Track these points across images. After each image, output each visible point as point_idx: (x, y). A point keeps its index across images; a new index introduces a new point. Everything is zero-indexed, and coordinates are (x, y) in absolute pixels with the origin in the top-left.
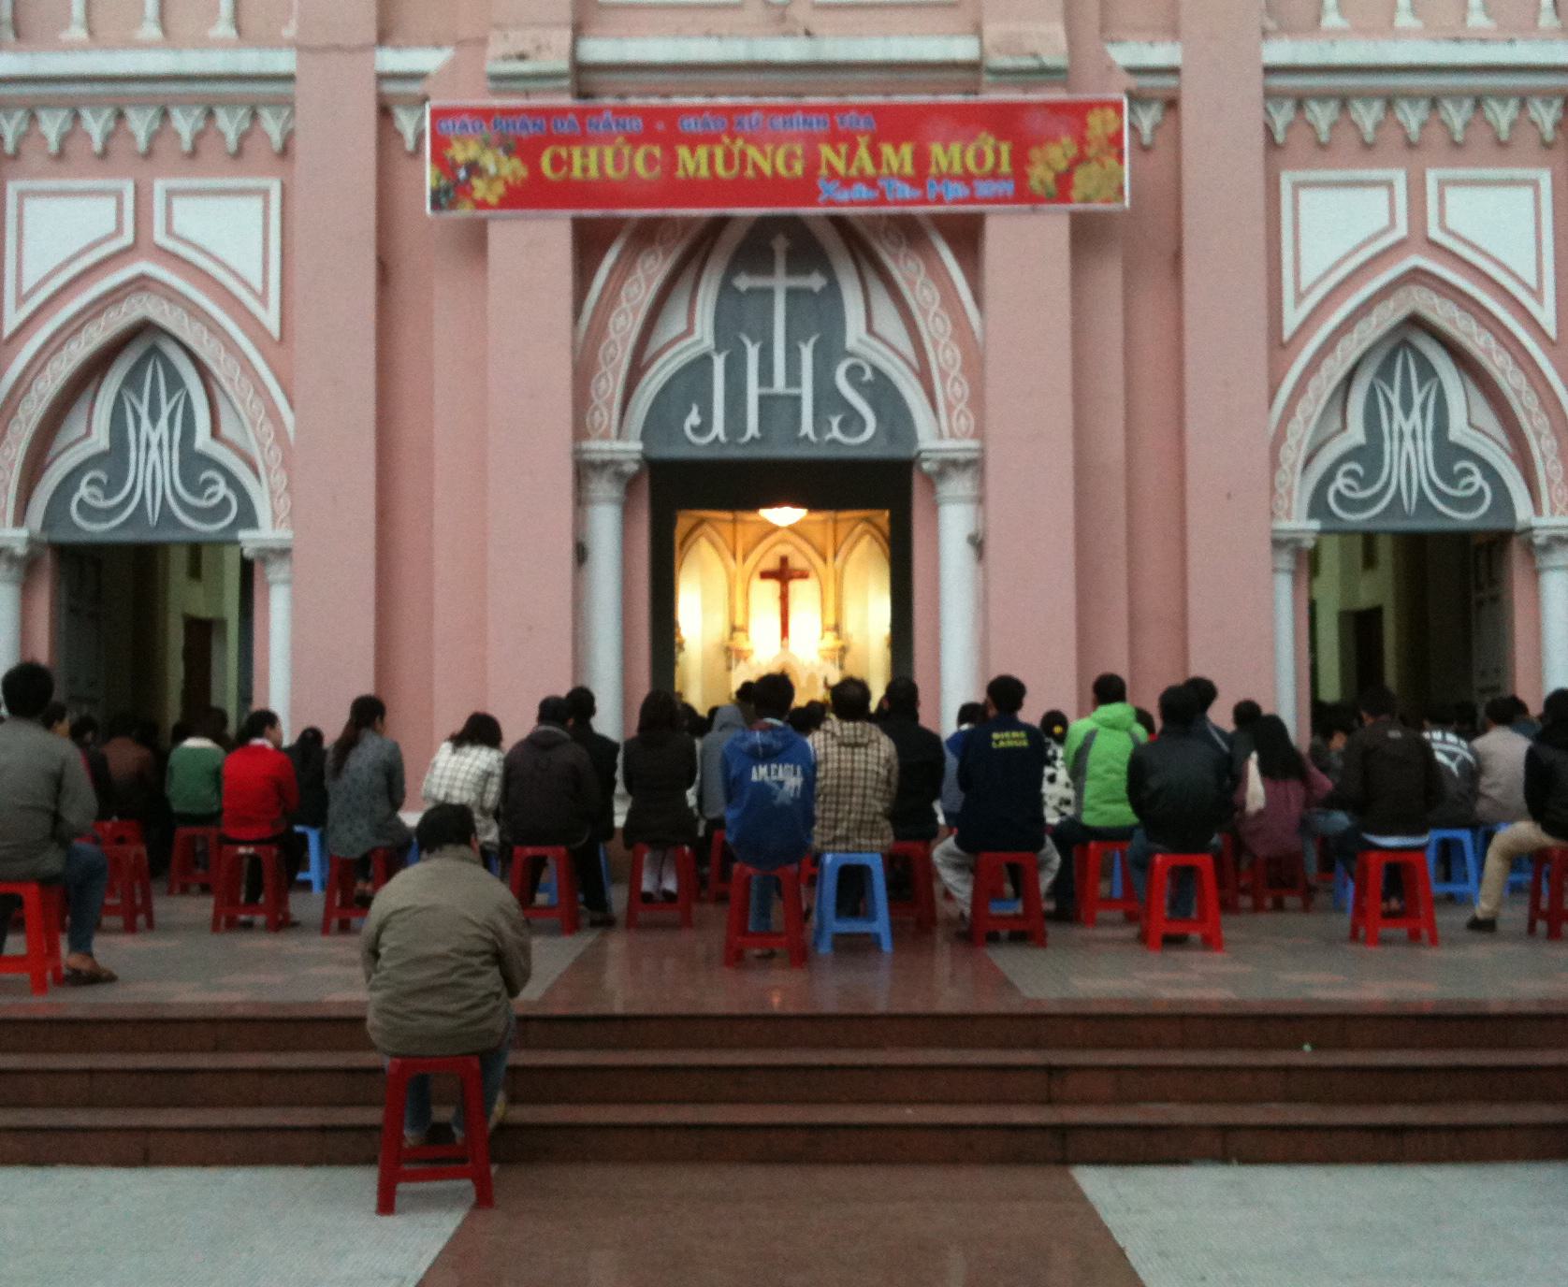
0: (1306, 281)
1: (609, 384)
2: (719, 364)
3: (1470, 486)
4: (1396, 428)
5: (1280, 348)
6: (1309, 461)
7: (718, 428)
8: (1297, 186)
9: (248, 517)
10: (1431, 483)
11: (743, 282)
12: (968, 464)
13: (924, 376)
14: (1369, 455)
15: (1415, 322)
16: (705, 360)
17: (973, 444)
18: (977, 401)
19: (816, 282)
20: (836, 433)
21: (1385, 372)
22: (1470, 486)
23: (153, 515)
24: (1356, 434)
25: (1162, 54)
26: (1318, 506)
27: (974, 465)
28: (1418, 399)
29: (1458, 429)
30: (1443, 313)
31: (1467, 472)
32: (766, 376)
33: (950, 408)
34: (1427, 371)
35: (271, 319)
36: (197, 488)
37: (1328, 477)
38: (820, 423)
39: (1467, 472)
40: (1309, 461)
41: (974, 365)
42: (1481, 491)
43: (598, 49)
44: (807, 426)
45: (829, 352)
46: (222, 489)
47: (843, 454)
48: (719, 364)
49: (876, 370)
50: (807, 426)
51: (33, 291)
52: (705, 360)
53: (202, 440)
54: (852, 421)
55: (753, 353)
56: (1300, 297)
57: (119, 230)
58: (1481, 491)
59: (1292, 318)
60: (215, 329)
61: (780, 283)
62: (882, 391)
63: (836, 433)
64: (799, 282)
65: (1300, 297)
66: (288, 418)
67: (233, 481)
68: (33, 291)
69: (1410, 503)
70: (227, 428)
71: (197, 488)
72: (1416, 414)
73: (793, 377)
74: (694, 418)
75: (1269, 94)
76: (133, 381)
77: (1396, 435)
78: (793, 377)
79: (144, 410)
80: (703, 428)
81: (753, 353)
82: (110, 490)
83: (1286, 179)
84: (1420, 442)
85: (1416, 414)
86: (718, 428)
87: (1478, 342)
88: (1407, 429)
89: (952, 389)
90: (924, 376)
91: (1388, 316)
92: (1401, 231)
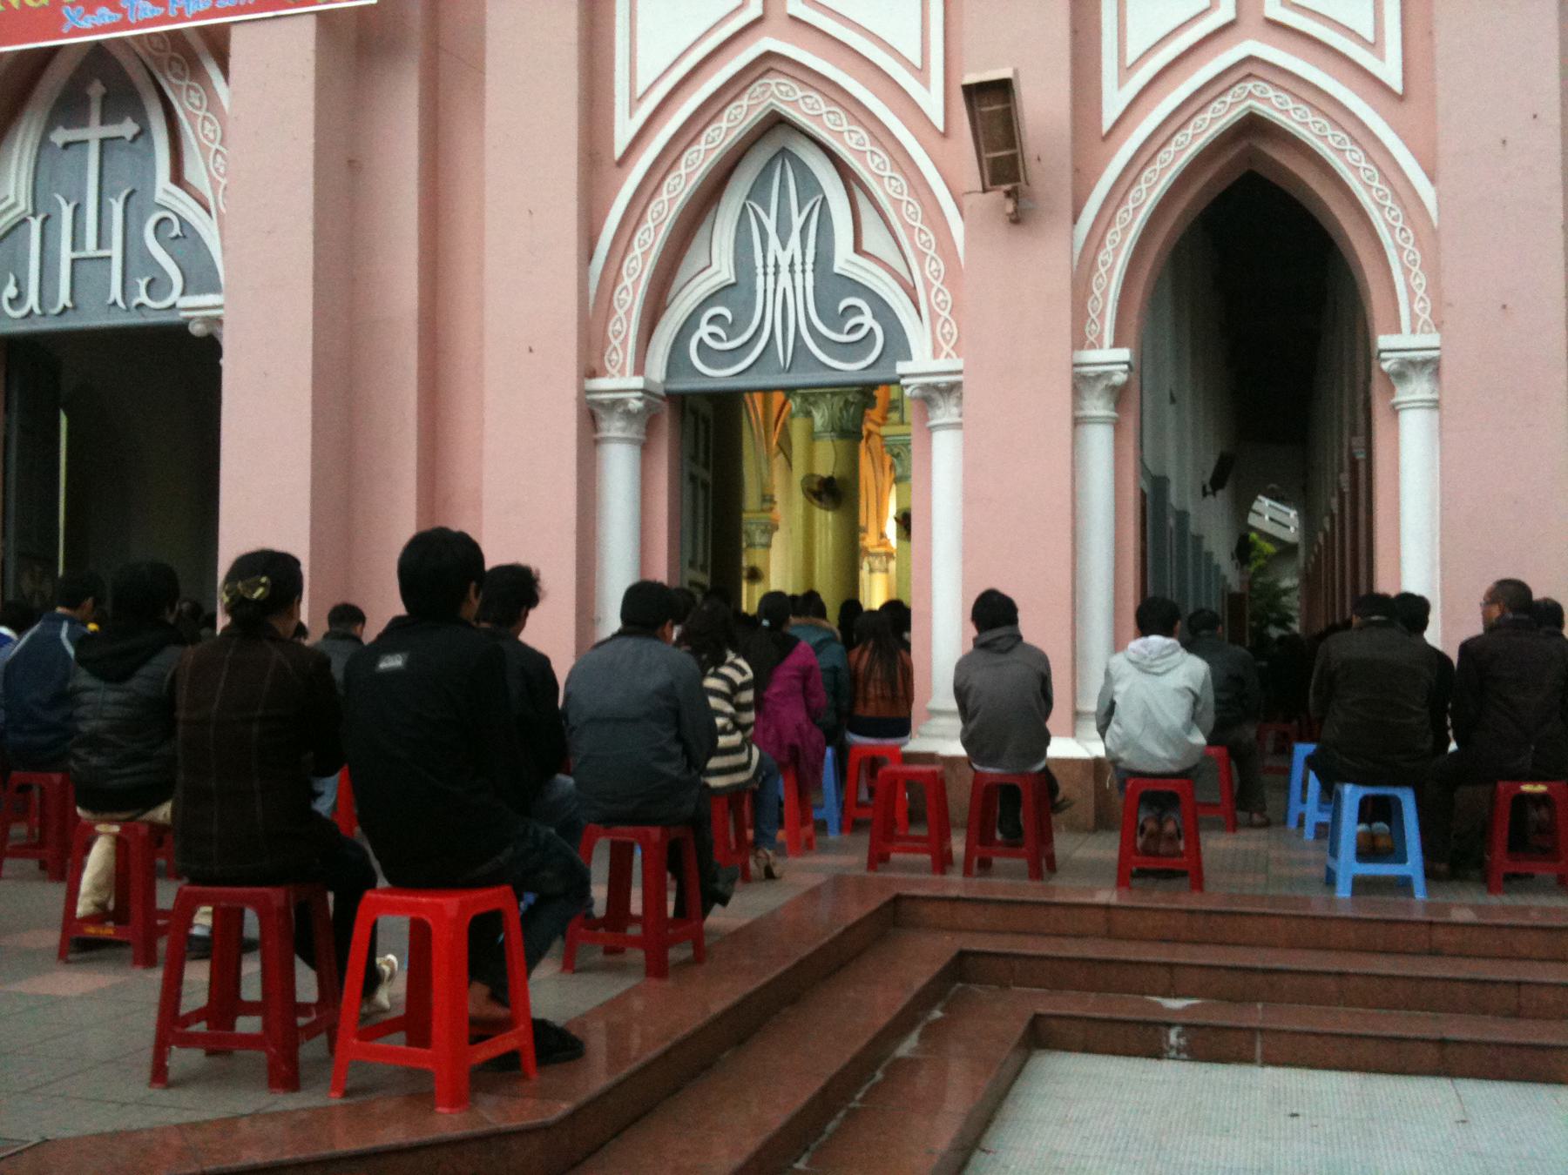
2: (35, 224)
3: (858, 326)
4: (771, 262)
7: (32, 300)
11: (60, 136)
14: (737, 293)
15: (775, 123)
19: (128, 128)
20: (143, 298)
21: (759, 191)
22: (858, 326)
24: (723, 270)
28: (797, 222)
29: (844, 260)
30: (804, 108)
31: (858, 311)
34: (808, 184)
37: (691, 323)
39: (853, 310)
42: (871, 330)
44: (116, 292)
47: (152, 319)
52: (25, 221)
54: (157, 285)
58: (871, 330)
61: (94, 133)
63: (143, 298)
64: (112, 131)
69: (784, 353)
74: (11, 291)
77: (771, 270)
80: (17, 301)
84: (798, 276)
86: (32, 300)
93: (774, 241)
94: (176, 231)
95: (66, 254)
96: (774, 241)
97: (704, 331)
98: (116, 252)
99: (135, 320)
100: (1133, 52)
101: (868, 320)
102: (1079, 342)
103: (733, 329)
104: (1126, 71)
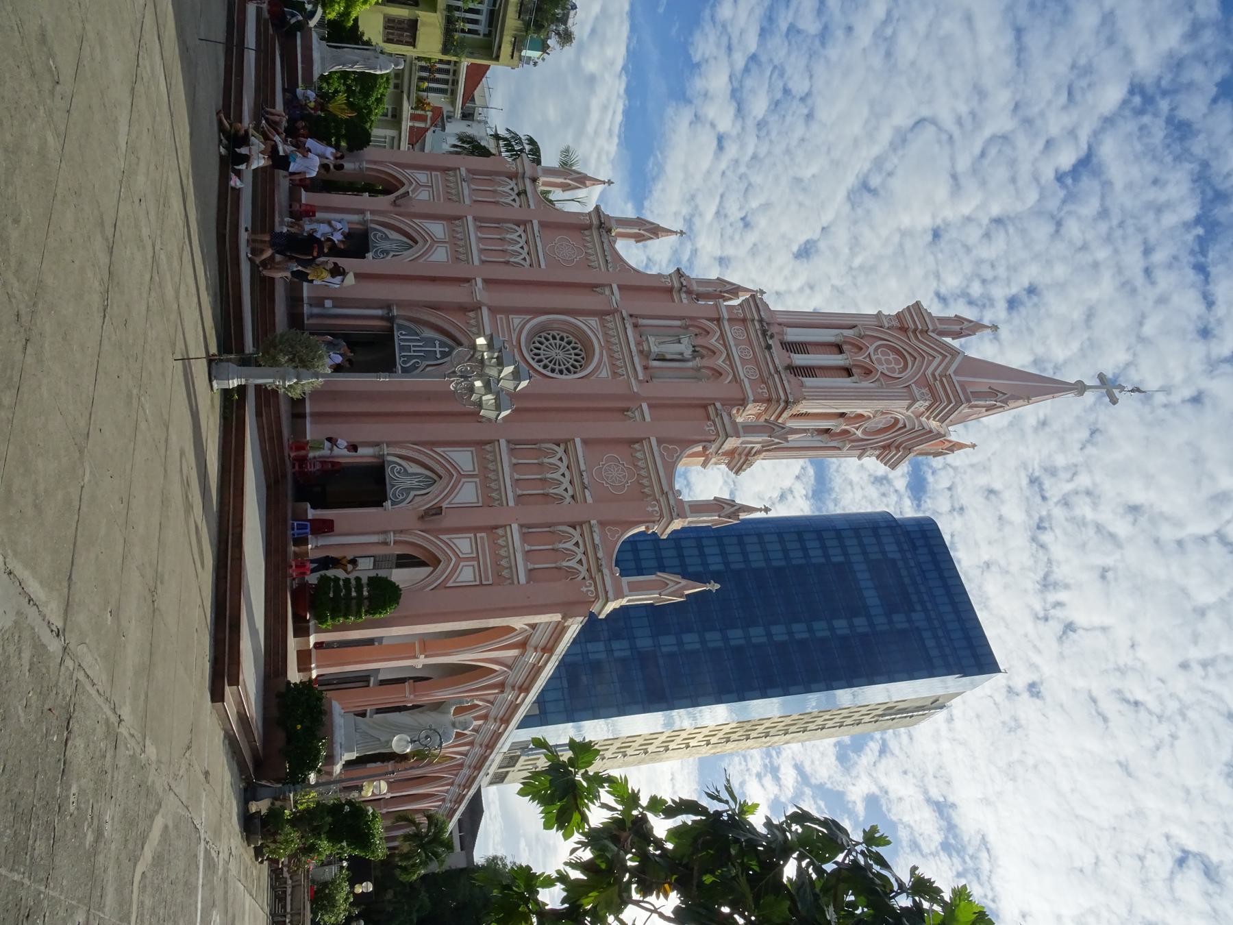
2: (418, 338)
7: (402, 337)
8: (472, 451)
11: (437, 343)
16: (418, 335)
32: (414, 346)
36: (382, 252)
38: (404, 356)
39: (403, 495)
43: (485, 311)
48: (418, 338)
54: (404, 362)
70: (418, 499)
73: (414, 351)
78: (414, 351)
80: (401, 334)
81: (421, 344)
86: (402, 337)
92: (463, 480)
95: (411, 344)
97: (398, 467)
98: (412, 354)
100: (454, 541)
101: (401, 498)
102: (395, 532)
103: (399, 473)
104: (450, 539)
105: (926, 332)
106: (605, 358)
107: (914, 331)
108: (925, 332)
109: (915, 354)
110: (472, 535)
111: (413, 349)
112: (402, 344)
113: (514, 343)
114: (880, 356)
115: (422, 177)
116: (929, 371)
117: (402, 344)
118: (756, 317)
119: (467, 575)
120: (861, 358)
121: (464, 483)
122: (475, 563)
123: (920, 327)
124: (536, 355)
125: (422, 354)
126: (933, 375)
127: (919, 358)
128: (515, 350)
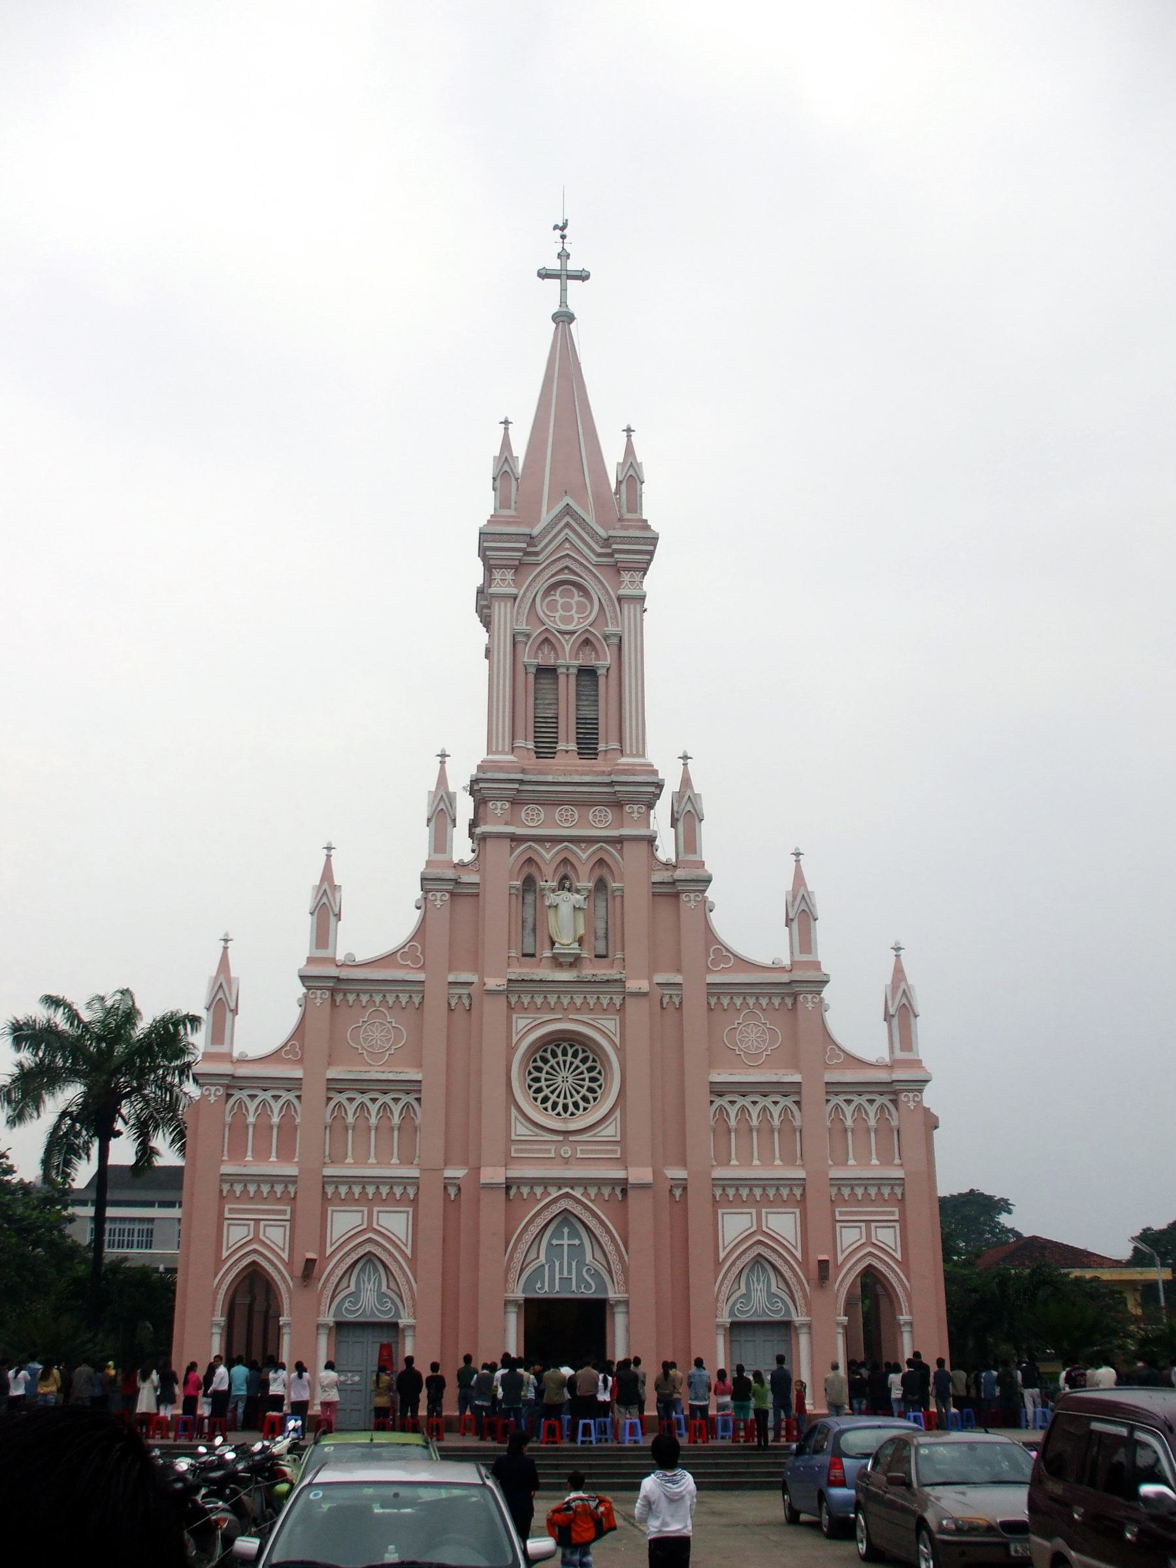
0: (726, 1243)
1: (513, 1275)
2: (547, 1267)
3: (778, 1306)
5: (718, 1264)
6: (728, 1299)
7: (546, 1288)
9: (397, 1314)
10: (767, 1307)
11: (555, 1242)
12: (624, 1301)
13: (610, 1272)
14: (747, 1296)
17: (626, 1295)
18: (626, 1283)
19: (577, 1242)
20: (583, 1290)
21: (752, 1270)
22: (778, 1306)
23: (368, 1313)
24: (743, 1290)
25: (681, 1173)
26: (732, 1313)
27: (626, 1303)
28: (762, 1279)
30: (767, 1254)
33: (618, 1283)
35: (408, 1252)
37: (735, 1304)
38: (578, 1287)
40: (728, 1299)
41: (625, 1270)
42: (781, 1308)
44: (574, 1288)
45: (581, 1263)
46: (390, 1305)
47: (585, 1296)
48: (547, 1267)
49: (595, 1270)
50: (574, 1288)
51: (796, 1244)
52: (543, 1265)
53: (384, 1288)
54: (588, 1286)
55: (557, 1264)
56: (724, 1248)
57: (378, 1225)
58: (781, 1308)
59: (722, 1255)
60: (391, 1254)
62: (596, 1275)
65: (724, 1248)
66: (414, 1285)
67: (393, 1302)
68: (796, 1244)
71: (382, 1304)
72: (761, 1284)
73: (570, 1272)
74: (539, 1285)
75: (714, 1185)
76: (362, 1270)
78: (570, 1272)
79: (366, 1279)
81: (557, 1264)
82: (355, 1304)
83: (720, 1211)
85: (761, 1284)
86: (546, 1288)
87: (779, 1263)
88: (759, 1289)
89: (618, 1277)
90: (610, 1272)
91: (751, 1254)
92: (754, 1228)
93: (756, 1283)
94: (593, 1272)
95: (557, 1277)
96: (756, 1283)
97: (738, 1305)
99: (579, 1296)
100: (844, 1247)
101: (780, 1304)
105: (531, 537)
106: (584, 1018)
107: (527, 554)
108: (531, 539)
109: (560, 565)
110: (838, 1225)
111: (565, 1275)
112: (557, 1288)
113: (561, 1138)
114: (557, 615)
115: (236, 1234)
116: (595, 559)
117: (557, 1288)
118: (516, 786)
119: (887, 1237)
120: (567, 648)
121: (752, 1225)
122: (873, 1225)
123: (524, 545)
124: (553, 1109)
125: (574, 1264)
126: (599, 555)
127: (567, 562)
128: (570, 1139)
